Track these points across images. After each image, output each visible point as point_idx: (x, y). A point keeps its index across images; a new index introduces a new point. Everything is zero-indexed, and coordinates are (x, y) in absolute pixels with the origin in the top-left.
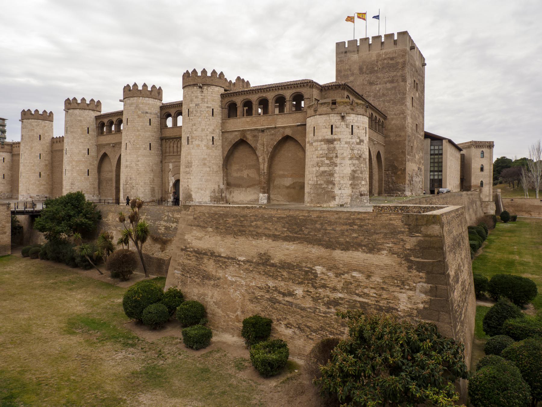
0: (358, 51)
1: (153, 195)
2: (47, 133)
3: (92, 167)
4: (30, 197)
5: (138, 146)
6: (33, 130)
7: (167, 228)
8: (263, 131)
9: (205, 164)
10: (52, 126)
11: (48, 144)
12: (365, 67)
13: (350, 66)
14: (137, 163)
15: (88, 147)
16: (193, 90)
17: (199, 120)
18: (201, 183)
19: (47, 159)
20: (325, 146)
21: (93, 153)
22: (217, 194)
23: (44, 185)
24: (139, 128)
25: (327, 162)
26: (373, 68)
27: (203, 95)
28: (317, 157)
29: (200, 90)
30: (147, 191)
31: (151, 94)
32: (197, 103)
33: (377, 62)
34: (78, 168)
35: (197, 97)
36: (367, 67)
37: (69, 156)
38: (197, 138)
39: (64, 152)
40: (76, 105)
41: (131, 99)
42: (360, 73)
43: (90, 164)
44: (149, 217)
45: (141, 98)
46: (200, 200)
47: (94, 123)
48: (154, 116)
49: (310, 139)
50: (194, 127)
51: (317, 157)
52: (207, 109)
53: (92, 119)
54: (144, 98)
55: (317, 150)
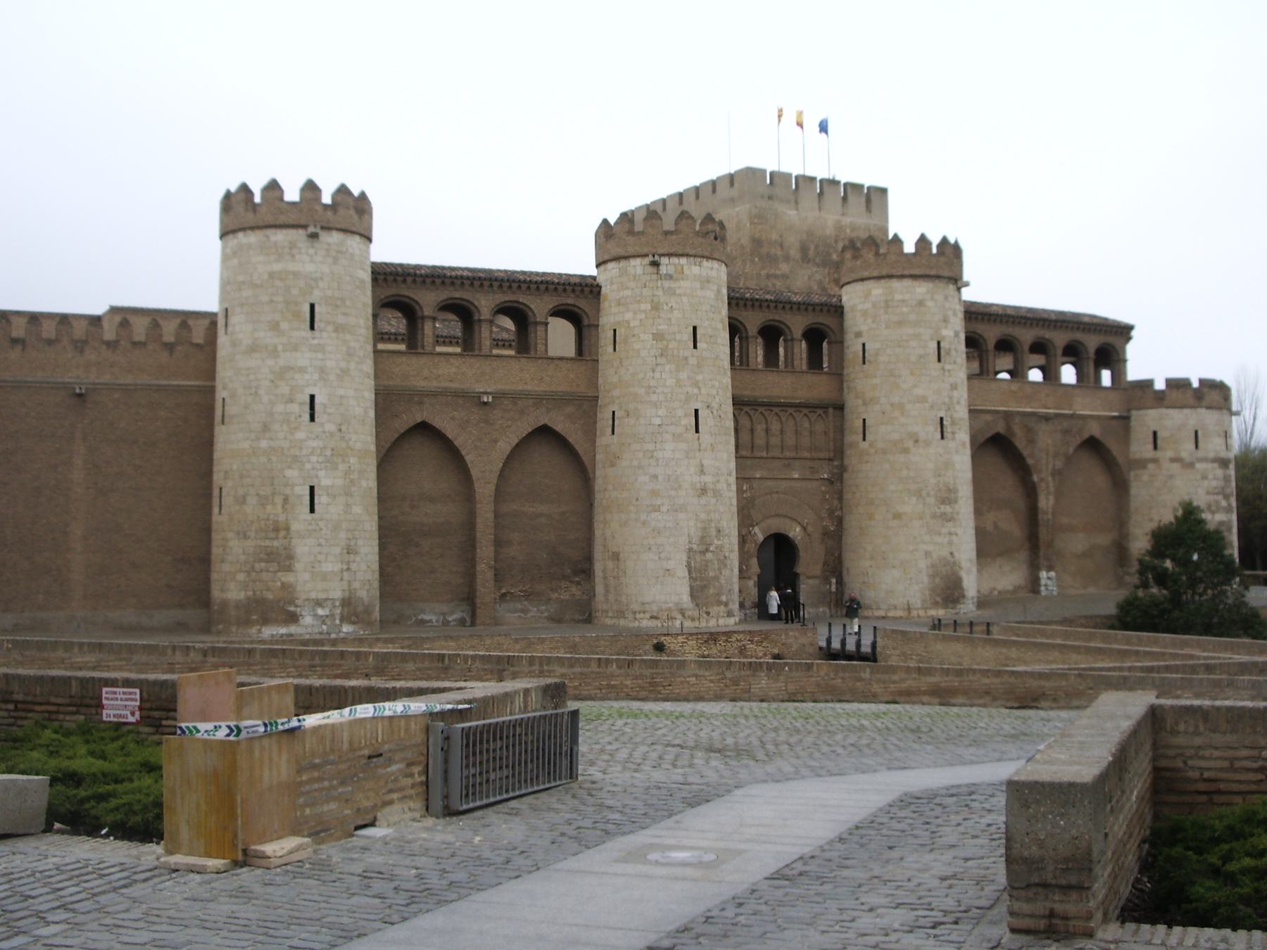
0: (796, 202)
8: (1047, 418)
12: (812, 247)
13: (781, 236)
20: (1220, 472)
25: (1224, 503)
26: (829, 254)
28: (1208, 493)
33: (836, 241)
34: (364, 484)
36: (817, 247)
37: (331, 427)
40: (356, 217)
41: (705, 263)
42: (803, 260)
49: (1184, 455)
51: (1208, 493)
55: (1204, 477)
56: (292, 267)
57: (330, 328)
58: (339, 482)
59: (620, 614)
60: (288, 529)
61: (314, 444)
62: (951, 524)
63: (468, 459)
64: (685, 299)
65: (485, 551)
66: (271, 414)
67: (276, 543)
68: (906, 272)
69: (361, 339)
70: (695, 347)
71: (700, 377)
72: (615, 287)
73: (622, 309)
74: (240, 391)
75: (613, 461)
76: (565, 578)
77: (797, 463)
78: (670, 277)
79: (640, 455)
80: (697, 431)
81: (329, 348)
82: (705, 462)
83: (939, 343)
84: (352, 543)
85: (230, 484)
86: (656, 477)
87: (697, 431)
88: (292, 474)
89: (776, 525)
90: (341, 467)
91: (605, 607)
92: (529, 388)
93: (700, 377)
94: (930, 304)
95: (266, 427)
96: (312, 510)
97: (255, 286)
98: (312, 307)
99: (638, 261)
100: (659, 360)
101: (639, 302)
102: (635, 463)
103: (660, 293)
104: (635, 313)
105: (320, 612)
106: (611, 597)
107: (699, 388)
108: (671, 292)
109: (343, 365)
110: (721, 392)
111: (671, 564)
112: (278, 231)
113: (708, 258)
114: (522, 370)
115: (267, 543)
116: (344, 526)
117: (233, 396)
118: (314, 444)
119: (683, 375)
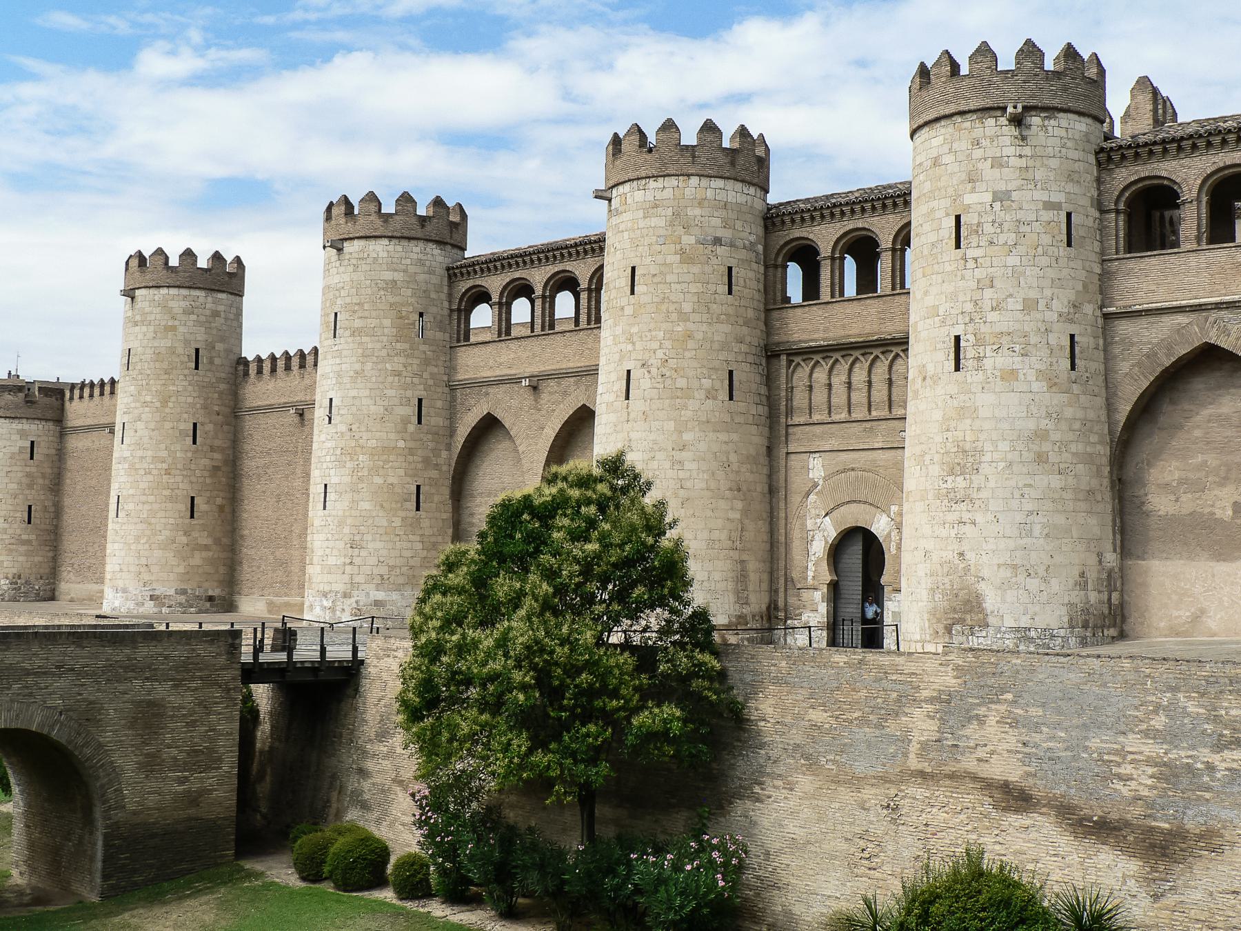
1: (742, 600)
2: (222, 339)
3: (434, 474)
4: (152, 598)
5: (681, 383)
6: (174, 328)
7: (1169, 773)
9: (1041, 459)
10: (239, 314)
11: (223, 386)
14: (678, 455)
15: (422, 394)
16: (978, 132)
17: (1013, 260)
18: (1027, 541)
19: (217, 443)
21: (434, 419)
22: (1093, 597)
23: (206, 548)
24: (687, 307)
27: (1027, 151)
29: (1013, 131)
30: (717, 576)
31: (733, 164)
32: (1002, 187)
34: (378, 480)
35: (998, 163)
37: (343, 428)
38: (1005, 340)
39: (320, 413)
41: (652, 184)
43: (426, 461)
44: (1036, 712)
45: (694, 181)
46: (1024, 622)
47: (444, 296)
48: (743, 254)
50: (988, 293)
52: (1047, 215)
53: (435, 280)
54: (705, 182)
57: (348, 333)
58: (348, 479)
62: (963, 506)
63: (521, 449)
68: (921, 121)
69: (385, 339)
70: (632, 292)
71: (635, 330)
77: (884, 424)
80: (627, 398)
81: (345, 353)
82: (634, 435)
83: (958, 218)
84: (357, 538)
87: (627, 398)
89: (854, 516)
90: (349, 465)
92: (571, 365)
93: (635, 330)
94: (947, 159)
105: (325, 603)
107: (634, 344)
109: (358, 367)
110: (668, 344)
113: (655, 177)
114: (566, 346)
116: (349, 521)
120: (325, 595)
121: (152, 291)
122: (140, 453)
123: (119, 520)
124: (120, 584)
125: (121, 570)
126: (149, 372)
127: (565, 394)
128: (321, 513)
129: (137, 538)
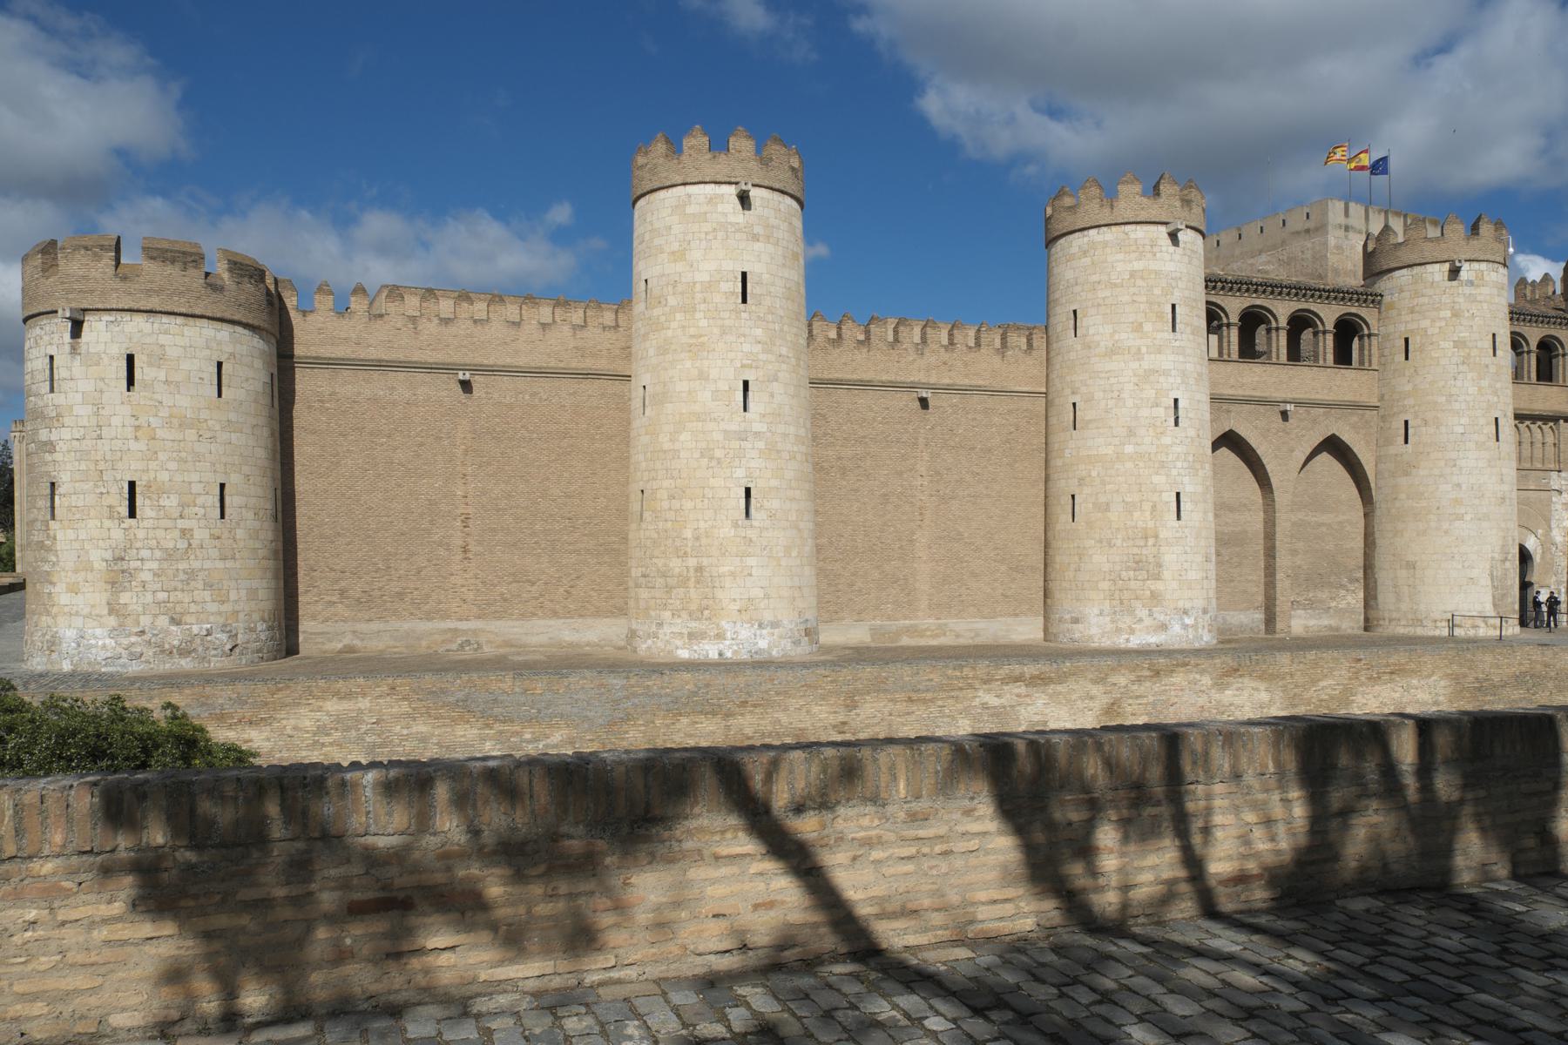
37: (1192, 433)
56: (1153, 266)
57: (1188, 330)
59: (1419, 622)
60: (1156, 537)
61: (1179, 449)
63: (1269, 468)
64: (1485, 306)
65: (1283, 560)
66: (1136, 418)
67: (1145, 552)
71: (1498, 385)
72: (1406, 294)
73: (1416, 316)
74: (1099, 395)
75: (1407, 469)
76: (1342, 586)
78: (1471, 283)
79: (1442, 463)
82: (1504, 471)
85: (1087, 490)
86: (1459, 485)
88: (1159, 480)
91: (1395, 615)
95: (1131, 432)
96: (1179, 517)
97: (1116, 285)
98: (1174, 306)
99: (1437, 266)
100: (1461, 368)
101: (1438, 309)
102: (1436, 472)
103: (1461, 300)
104: (1433, 321)
105: (1188, 621)
106: (1404, 606)
108: (1472, 299)
111: (1475, 573)
112: (1139, 227)
115: (1136, 550)
117: (1089, 399)
118: (1179, 449)
119: (1485, 383)
120: (1185, 612)
121: (777, 196)
122: (781, 428)
123: (755, 523)
124: (768, 616)
125: (767, 597)
126: (781, 313)
127: (1314, 421)
128: (1176, 524)
129: (788, 549)
